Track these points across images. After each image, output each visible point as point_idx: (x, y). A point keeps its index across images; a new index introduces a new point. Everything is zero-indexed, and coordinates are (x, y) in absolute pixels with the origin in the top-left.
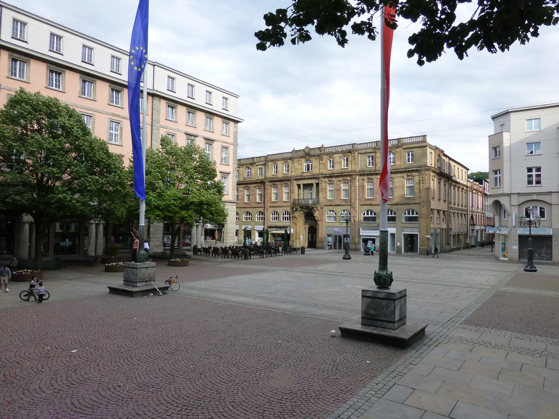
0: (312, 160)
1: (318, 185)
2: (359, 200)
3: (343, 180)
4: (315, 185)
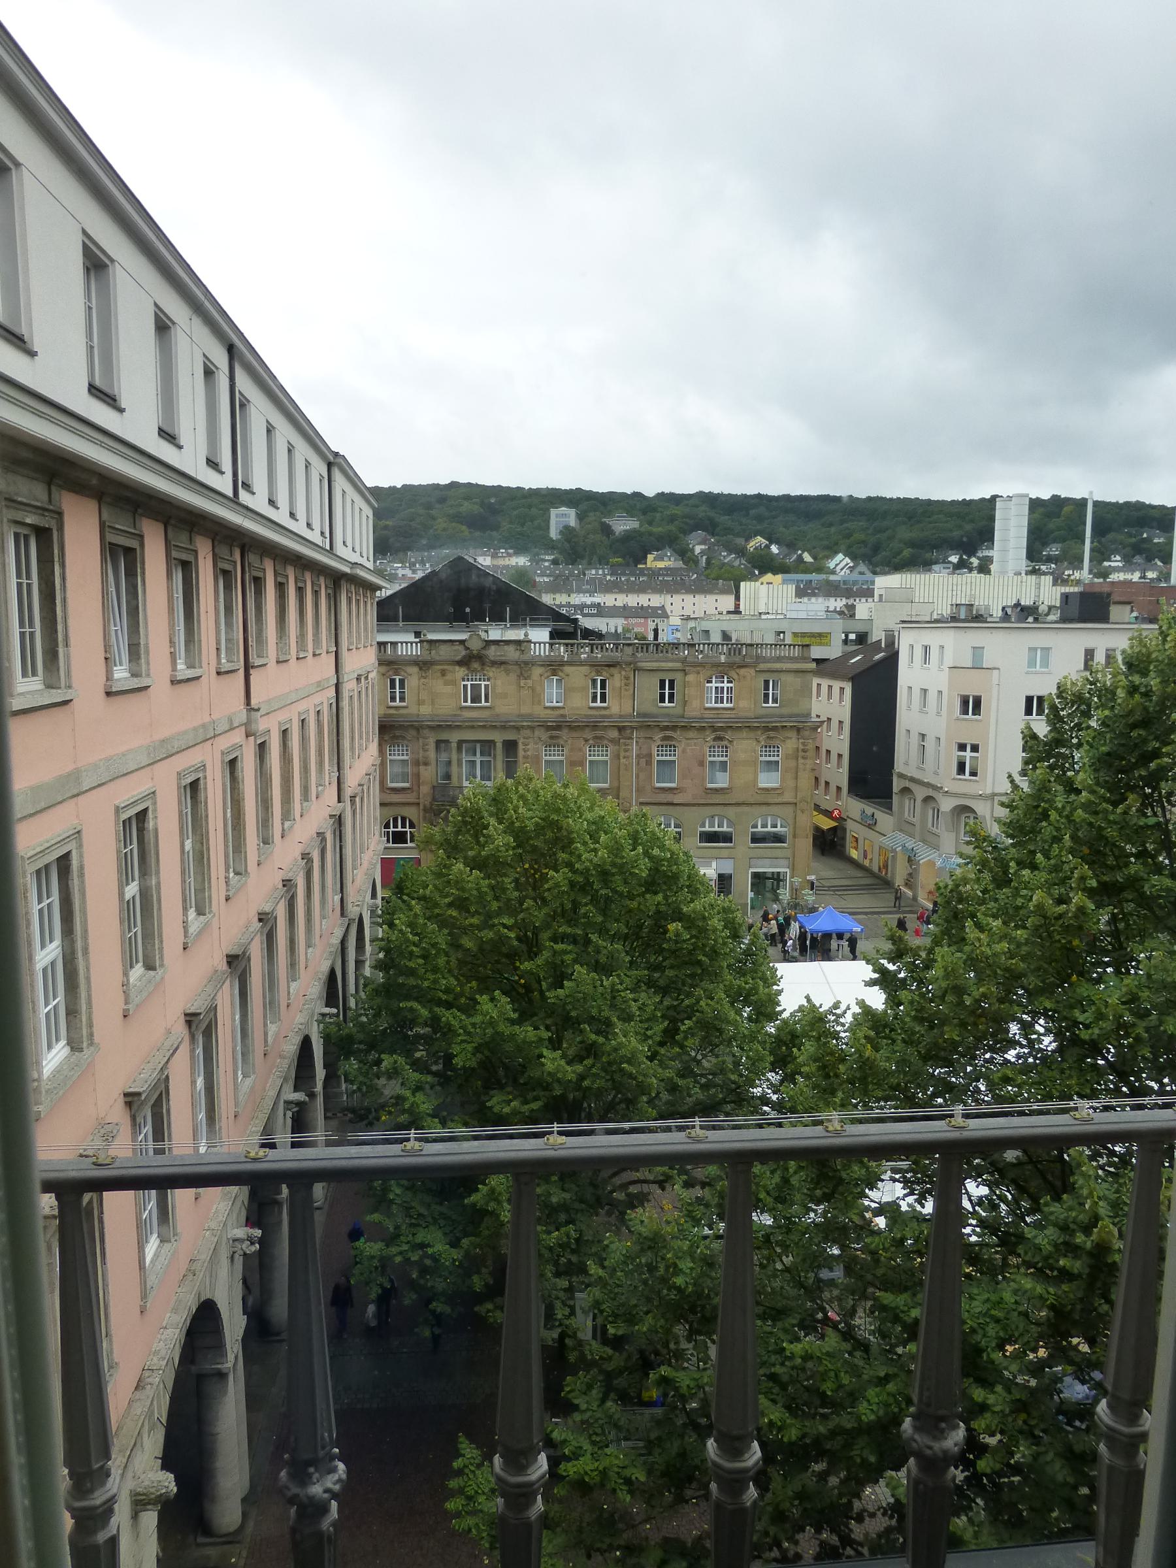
0: (491, 674)
1: (511, 747)
2: (638, 790)
3: (596, 738)
4: (499, 746)
